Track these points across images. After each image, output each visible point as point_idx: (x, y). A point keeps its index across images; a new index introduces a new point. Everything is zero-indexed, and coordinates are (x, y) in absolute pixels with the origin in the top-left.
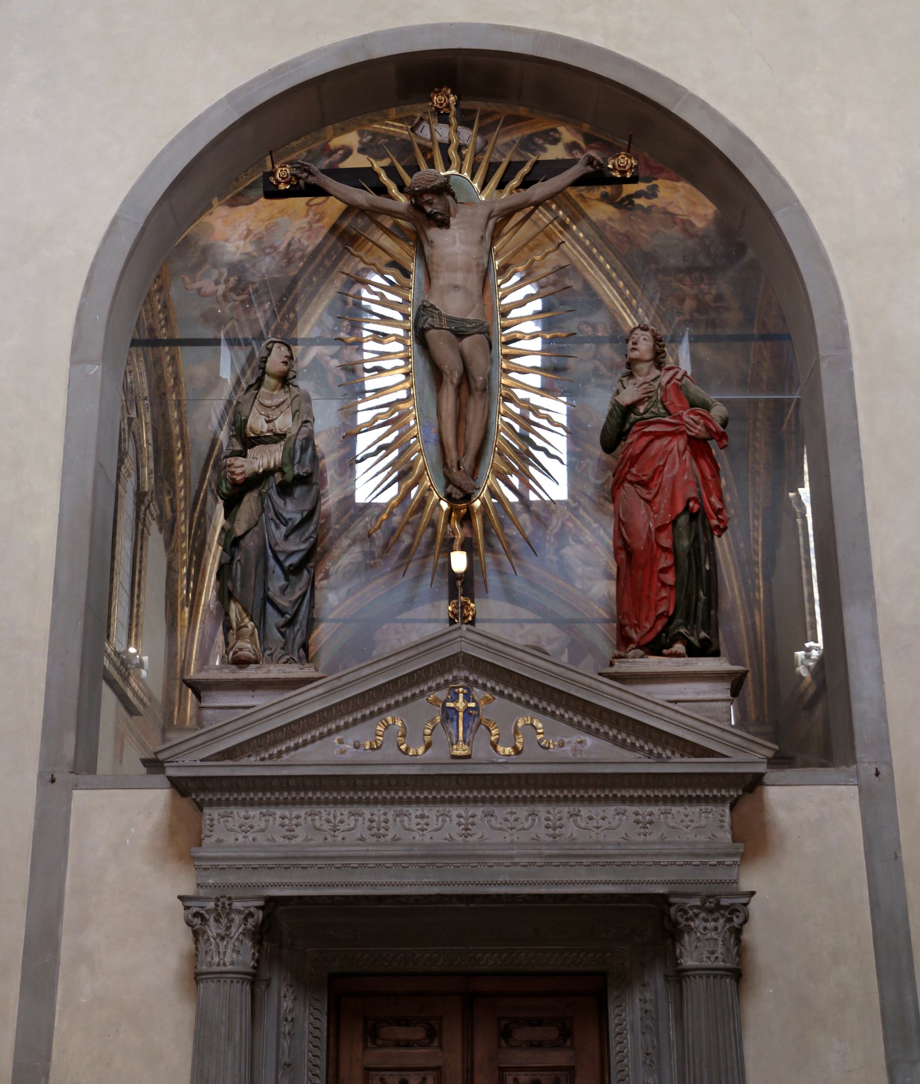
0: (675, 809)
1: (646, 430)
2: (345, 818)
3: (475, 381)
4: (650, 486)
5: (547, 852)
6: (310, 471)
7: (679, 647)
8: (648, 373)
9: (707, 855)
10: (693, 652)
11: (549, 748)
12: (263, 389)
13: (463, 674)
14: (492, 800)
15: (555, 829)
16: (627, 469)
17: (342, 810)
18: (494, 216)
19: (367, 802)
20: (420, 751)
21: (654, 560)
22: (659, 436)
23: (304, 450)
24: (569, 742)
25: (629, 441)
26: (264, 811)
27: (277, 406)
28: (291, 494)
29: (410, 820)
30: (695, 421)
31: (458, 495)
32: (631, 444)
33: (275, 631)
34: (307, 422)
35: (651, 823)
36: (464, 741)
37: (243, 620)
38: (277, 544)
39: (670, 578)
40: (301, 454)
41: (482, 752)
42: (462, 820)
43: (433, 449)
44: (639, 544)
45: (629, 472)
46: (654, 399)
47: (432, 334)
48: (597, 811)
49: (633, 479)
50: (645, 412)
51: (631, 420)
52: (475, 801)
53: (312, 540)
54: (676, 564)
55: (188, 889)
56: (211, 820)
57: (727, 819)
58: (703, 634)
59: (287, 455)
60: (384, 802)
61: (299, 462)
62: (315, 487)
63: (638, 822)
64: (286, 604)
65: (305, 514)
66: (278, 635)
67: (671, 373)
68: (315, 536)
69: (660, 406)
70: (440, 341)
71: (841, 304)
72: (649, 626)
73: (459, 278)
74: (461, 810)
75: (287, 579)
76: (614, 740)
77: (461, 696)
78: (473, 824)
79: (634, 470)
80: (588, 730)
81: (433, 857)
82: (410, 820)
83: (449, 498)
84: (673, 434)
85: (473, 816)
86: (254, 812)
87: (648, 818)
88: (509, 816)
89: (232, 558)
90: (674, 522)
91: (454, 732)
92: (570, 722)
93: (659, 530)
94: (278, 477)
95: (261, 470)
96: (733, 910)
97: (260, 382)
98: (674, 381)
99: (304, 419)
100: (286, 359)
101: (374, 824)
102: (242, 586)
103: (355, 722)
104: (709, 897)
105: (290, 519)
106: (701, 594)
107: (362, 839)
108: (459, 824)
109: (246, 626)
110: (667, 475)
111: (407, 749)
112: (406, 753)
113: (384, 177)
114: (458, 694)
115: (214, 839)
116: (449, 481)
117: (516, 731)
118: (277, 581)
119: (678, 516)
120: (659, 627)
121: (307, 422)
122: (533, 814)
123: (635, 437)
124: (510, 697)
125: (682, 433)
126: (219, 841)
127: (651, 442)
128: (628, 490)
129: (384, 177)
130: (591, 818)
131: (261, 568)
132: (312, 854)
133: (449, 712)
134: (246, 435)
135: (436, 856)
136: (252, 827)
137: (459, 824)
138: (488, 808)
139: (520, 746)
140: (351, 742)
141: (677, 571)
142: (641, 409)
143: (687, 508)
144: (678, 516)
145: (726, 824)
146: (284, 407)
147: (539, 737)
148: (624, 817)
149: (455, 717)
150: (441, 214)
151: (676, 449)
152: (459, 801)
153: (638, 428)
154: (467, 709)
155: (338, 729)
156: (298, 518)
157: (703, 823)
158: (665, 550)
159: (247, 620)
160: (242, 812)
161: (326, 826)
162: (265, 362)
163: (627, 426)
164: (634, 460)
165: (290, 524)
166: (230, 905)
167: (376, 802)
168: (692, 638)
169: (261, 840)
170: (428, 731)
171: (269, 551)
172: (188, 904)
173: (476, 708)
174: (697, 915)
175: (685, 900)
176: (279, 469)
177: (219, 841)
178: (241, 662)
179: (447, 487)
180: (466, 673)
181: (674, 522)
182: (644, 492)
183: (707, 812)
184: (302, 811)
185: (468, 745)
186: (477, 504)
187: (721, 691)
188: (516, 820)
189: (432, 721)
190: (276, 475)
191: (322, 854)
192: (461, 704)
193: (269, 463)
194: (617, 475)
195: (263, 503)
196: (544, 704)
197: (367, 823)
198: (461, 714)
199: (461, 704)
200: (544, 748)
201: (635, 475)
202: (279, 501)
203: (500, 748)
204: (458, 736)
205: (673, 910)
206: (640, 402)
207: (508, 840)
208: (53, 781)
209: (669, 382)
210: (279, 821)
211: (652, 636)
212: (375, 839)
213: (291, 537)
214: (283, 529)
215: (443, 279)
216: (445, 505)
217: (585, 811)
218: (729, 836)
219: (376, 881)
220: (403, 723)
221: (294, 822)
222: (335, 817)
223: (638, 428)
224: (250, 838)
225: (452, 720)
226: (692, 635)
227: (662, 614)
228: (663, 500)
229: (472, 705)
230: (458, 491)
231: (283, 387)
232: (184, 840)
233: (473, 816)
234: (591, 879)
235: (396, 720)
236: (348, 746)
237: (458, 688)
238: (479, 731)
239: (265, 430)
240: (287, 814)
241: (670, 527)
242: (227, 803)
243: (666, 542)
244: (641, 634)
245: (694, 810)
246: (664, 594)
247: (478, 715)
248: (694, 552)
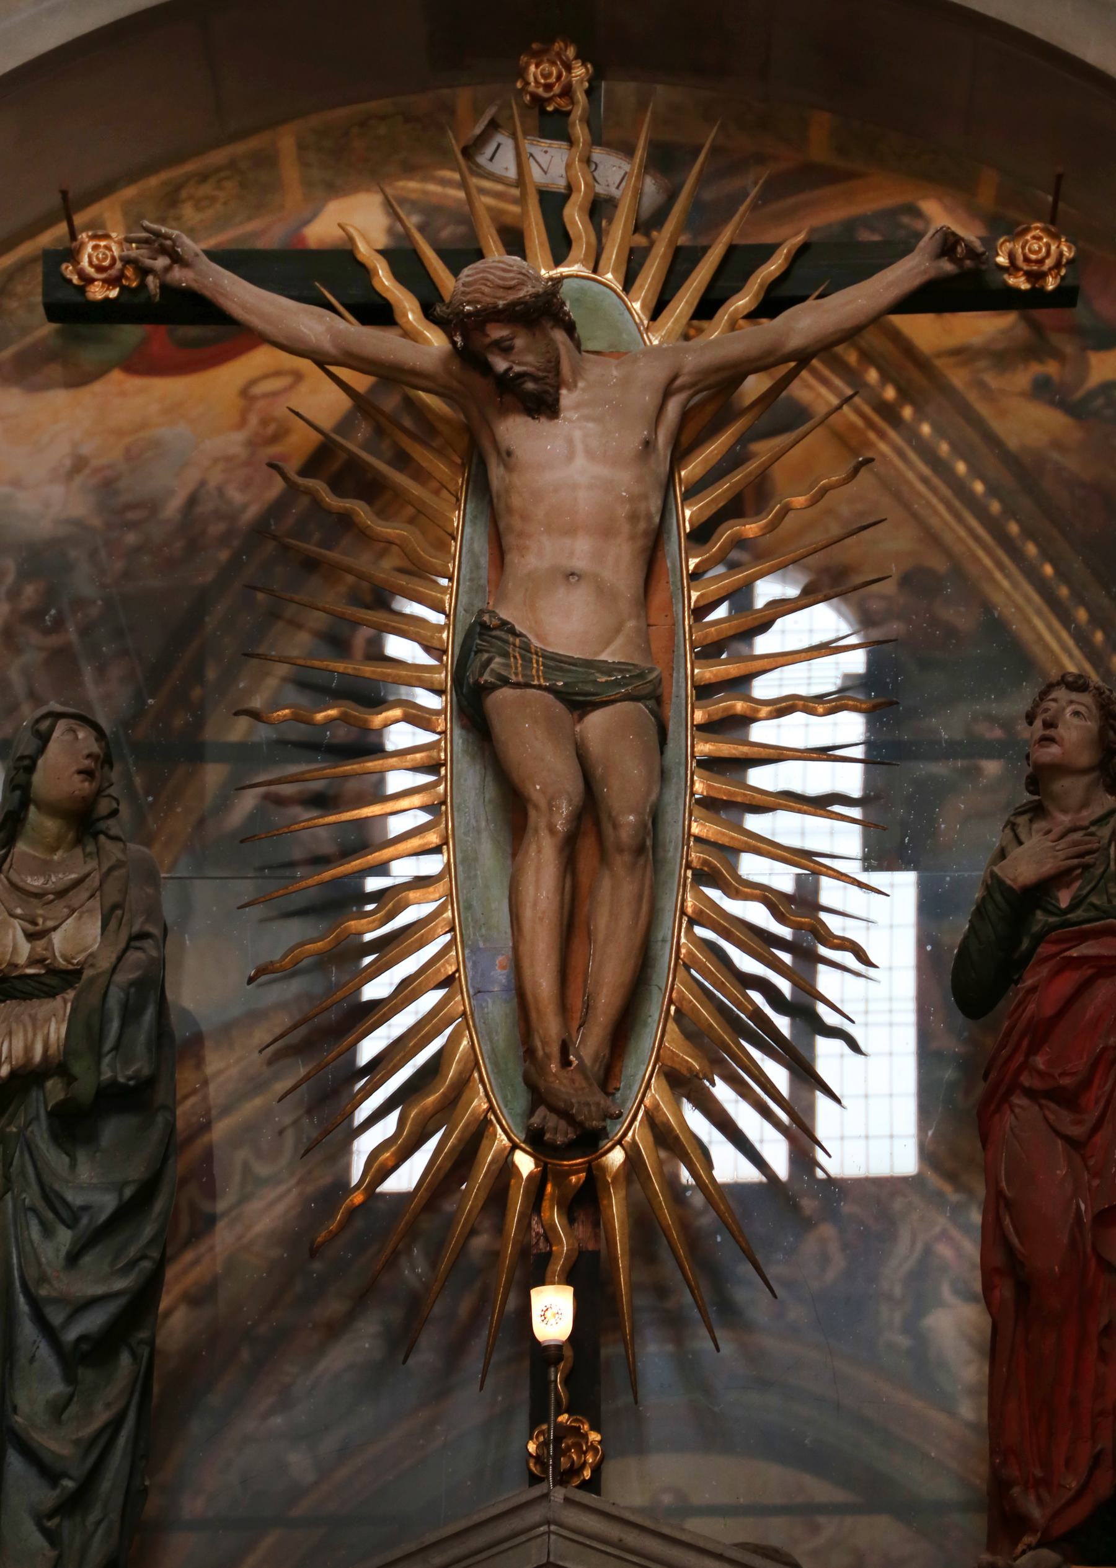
1: (1074, 953)
3: (616, 826)
6: (146, 1072)
16: (1020, 1058)
23: (130, 1014)
25: (1029, 982)
28: (90, 1139)
31: (560, 1133)
32: (1033, 990)
34: (143, 936)
38: (43, 1279)
43: (498, 1010)
45: (1024, 1066)
49: (1036, 1083)
51: (1036, 928)
53: (146, 1265)
61: (116, 1048)
62: (160, 1119)
65: (128, 1192)
68: (155, 1254)
73: (580, 551)
75: (70, 1378)
79: (1039, 1061)
83: (536, 1142)
99: (136, 928)
105: (85, 1208)
113: (384, 279)
116: (538, 1096)
121: (143, 936)
123: (1044, 971)
128: (1022, 1116)
129: (384, 279)
153: (1054, 949)
156: (108, 1203)
163: (1025, 944)
164: (1040, 1032)
165: (84, 1221)
171: (22, 1299)
176: (56, 1067)
179: (531, 1112)
182: (1065, 1121)
190: (49, 1084)
194: (992, 1076)
201: (1041, 1074)
202: (54, 1158)
213: (87, 1259)
214: (65, 1237)
223: (1054, 949)
230: (563, 1124)
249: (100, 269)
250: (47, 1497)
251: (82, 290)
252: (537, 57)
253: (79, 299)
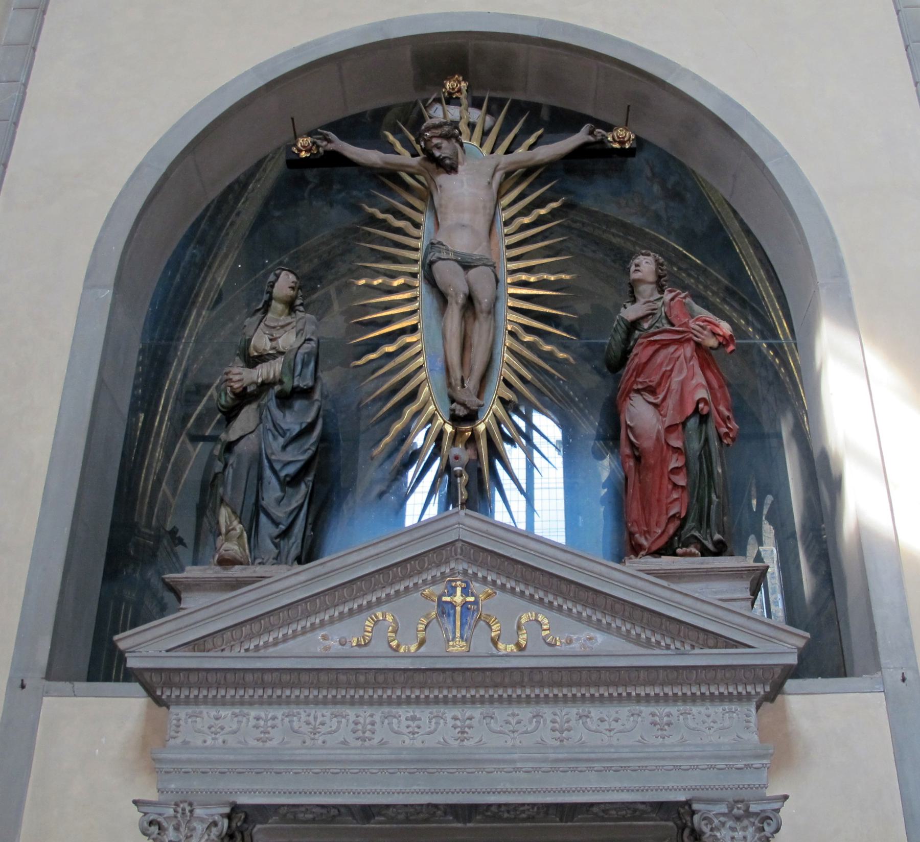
0: (695, 710)
2: (327, 719)
3: (480, 304)
4: (658, 391)
5: (553, 756)
6: (310, 384)
8: (651, 295)
9: (733, 757)
11: (555, 645)
12: (270, 315)
14: (491, 700)
15: (562, 732)
16: (633, 379)
17: (324, 711)
18: (500, 169)
19: (352, 702)
20: (413, 648)
21: (664, 461)
22: (665, 344)
23: (305, 364)
24: (578, 639)
26: (237, 711)
27: (282, 327)
28: (290, 407)
29: (399, 722)
30: (701, 327)
32: (637, 354)
33: (268, 542)
35: (669, 724)
36: (462, 637)
37: (231, 523)
40: (302, 368)
42: (458, 723)
44: (647, 444)
46: (658, 315)
47: (438, 267)
48: (610, 711)
49: (640, 387)
50: (650, 328)
52: (473, 701)
54: (686, 464)
55: (151, 795)
56: (179, 720)
57: (753, 718)
58: (717, 536)
59: (287, 365)
60: (371, 702)
61: (300, 375)
63: (654, 724)
64: (281, 515)
65: (304, 426)
66: (272, 546)
67: (673, 294)
69: (664, 321)
71: (834, 239)
72: (660, 530)
73: (466, 218)
74: (457, 711)
76: (627, 637)
77: (459, 590)
78: (470, 727)
79: (640, 380)
80: (598, 626)
81: (424, 762)
82: (399, 722)
85: (470, 718)
86: (225, 712)
87: (665, 719)
88: (510, 719)
90: (684, 424)
91: (450, 628)
92: (579, 618)
93: (670, 429)
94: (277, 388)
95: (260, 380)
96: (765, 818)
97: (267, 307)
98: (677, 299)
100: (293, 285)
101: (360, 727)
102: (233, 489)
104: (737, 802)
105: (288, 430)
106: (714, 497)
107: (345, 742)
108: (455, 727)
109: (234, 529)
110: (676, 379)
111: (398, 646)
114: (455, 587)
115: (179, 741)
117: (519, 628)
118: (272, 491)
119: (688, 418)
120: (671, 529)
122: (538, 716)
125: (689, 340)
126: (185, 743)
127: (656, 351)
130: (602, 720)
131: (254, 473)
132: (287, 758)
133: (445, 606)
134: (249, 354)
135: (427, 761)
136: (222, 728)
137: (455, 727)
138: (487, 709)
139: (523, 643)
140: (337, 638)
142: (646, 326)
143: (696, 411)
144: (688, 418)
145: (752, 725)
146: (290, 327)
147: (544, 633)
148: (640, 719)
149: (452, 612)
150: (450, 159)
151: (682, 356)
152: (455, 701)
154: (465, 604)
155: (322, 624)
156: (296, 429)
157: (727, 723)
158: (676, 450)
159: (235, 523)
160: (213, 712)
161: (305, 729)
162: (272, 287)
164: (640, 369)
165: (288, 434)
166: (191, 811)
167: (362, 702)
168: (706, 542)
169: (232, 742)
170: (421, 627)
172: (146, 809)
173: (476, 603)
174: (723, 824)
175: (709, 807)
177: (185, 743)
178: (225, 562)
180: (465, 566)
181: (684, 424)
182: (651, 399)
183: (730, 711)
184: (279, 712)
186: (481, 427)
187: (742, 589)
188: (519, 722)
189: (427, 616)
191: (298, 758)
192: (458, 598)
193: (268, 373)
195: (261, 414)
196: (551, 597)
197: (352, 726)
198: (458, 609)
200: (549, 644)
203: (501, 646)
204: (454, 633)
205: (696, 818)
206: (645, 317)
207: (510, 743)
208: (23, 687)
209: (672, 299)
210: (253, 722)
211: (665, 539)
212: (359, 743)
213: (289, 449)
214: (281, 441)
215: (450, 219)
216: (449, 429)
217: (595, 712)
218: (756, 737)
219: (359, 788)
220: (394, 619)
221: (270, 723)
222: (315, 718)
224: (220, 741)
225: (449, 615)
226: (706, 539)
227: (674, 516)
228: (671, 402)
229: (472, 599)
230: (462, 408)
231: (289, 314)
232: (152, 752)
233: (470, 718)
234: (604, 786)
235: (387, 616)
236: (334, 643)
237: (455, 581)
238: (478, 627)
239: (268, 348)
240: (263, 715)
241: (680, 427)
242: (196, 701)
244: (651, 539)
245: (716, 710)
246: (675, 496)
247: (478, 609)
248: (706, 453)
249: (304, 147)
250: (276, 531)
251: (298, 155)
252: (449, 80)
253: (297, 158)
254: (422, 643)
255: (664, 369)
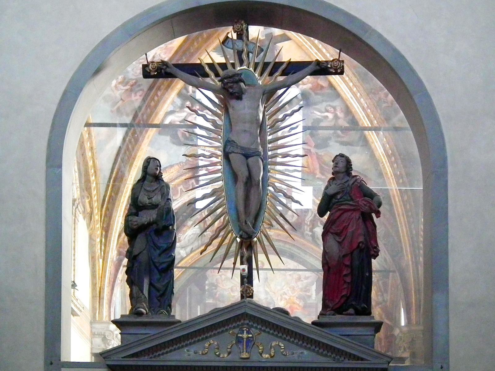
7: (351, 311)
8: (343, 179)
10: (358, 313)
11: (286, 355)
13: (247, 322)
20: (226, 356)
21: (341, 271)
24: (296, 353)
27: (153, 191)
36: (246, 352)
39: (348, 279)
41: (255, 357)
43: (233, 213)
46: (345, 192)
50: (341, 198)
69: (348, 195)
70: (236, 159)
76: (318, 353)
77: (245, 331)
80: (305, 348)
84: (354, 210)
89: (133, 265)
90: (352, 253)
93: (344, 256)
94: (155, 226)
95: (146, 223)
103: (194, 342)
110: (350, 230)
111: (220, 354)
112: (219, 356)
117: (271, 348)
124: (269, 333)
139: (272, 354)
141: (352, 275)
142: (339, 197)
143: (358, 246)
144: (354, 250)
146: (157, 191)
147: (282, 350)
149: (242, 341)
155: (187, 345)
158: (347, 266)
163: (331, 205)
170: (230, 347)
176: (155, 222)
181: (352, 253)
182: (337, 239)
185: (248, 353)
198: (245, 340)
199: (245, 335)
200: (284, 355)
203: (264, 355)
220: (217, 343)
227: (343, 296)
229: (250, 336)
231: (156, 181)
236: (192, 353)
237: (244, 328)
238: (253, 347)
239: (147, 203)
243: (348, 263)
247: (253, 340)
254: (229, 353)
255: (344, 225)
